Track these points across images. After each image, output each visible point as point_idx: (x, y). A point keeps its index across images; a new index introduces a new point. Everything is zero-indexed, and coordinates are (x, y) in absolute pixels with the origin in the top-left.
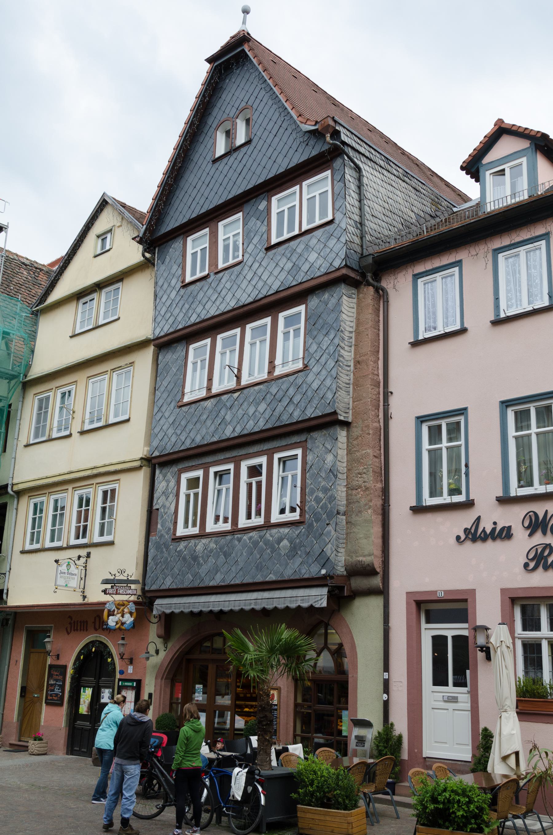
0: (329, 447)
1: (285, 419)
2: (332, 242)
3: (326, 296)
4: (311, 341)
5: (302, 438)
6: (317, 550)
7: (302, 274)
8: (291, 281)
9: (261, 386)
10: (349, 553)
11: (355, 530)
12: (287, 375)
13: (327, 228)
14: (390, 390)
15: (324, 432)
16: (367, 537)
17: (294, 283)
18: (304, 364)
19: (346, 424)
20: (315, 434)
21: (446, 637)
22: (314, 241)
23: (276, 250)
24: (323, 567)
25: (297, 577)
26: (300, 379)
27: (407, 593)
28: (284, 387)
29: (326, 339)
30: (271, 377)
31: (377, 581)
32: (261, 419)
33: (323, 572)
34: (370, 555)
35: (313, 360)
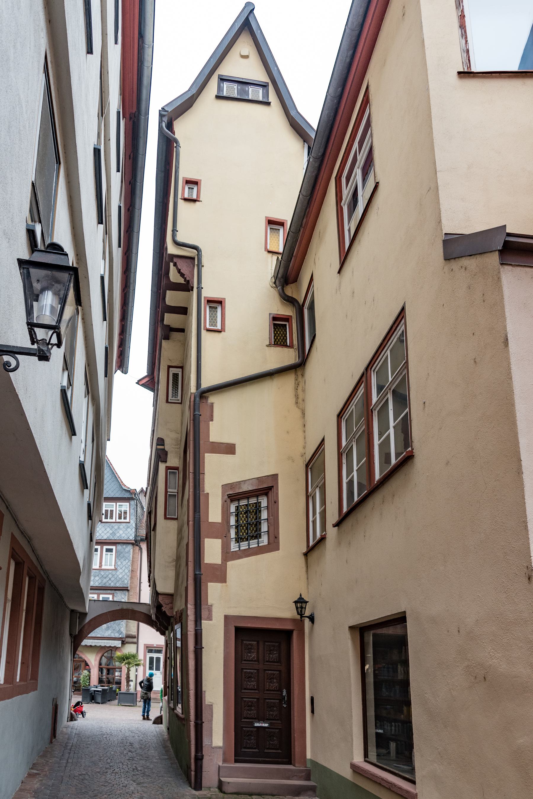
0: (123, 597)
1: (107, 585)
2: (129, 530)
3: (124, 546)
4: (118, 560)
5: (113, 592)
6: (117, 629)
7: (117, 537)
8: (111, 538)
9: (97, 571)
10: (127, 631)
11: (130, 624)
12: (108, 570)
13: (127, 524)
14: (141, 581)
15: (121, 592)
16: (134, 627)
17: (113, 539)
18: (115, 567)
19: (128, 590)
20: (117, 592)
21: (154, 657)
22: (121, 527)
23: (105, 524)
24: (120, 634)
25: (110, 637)
26: (114, 572)
27: (144, 644)
28: (107, 573)
29: (124, 561)
30: (100, 568)
31: (135, 640)
32: (97, 582)
33: (121, 636)
34: (135, 632)
35: (119, 567)
